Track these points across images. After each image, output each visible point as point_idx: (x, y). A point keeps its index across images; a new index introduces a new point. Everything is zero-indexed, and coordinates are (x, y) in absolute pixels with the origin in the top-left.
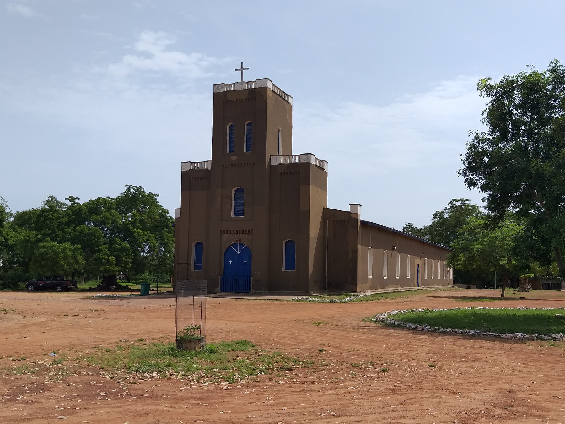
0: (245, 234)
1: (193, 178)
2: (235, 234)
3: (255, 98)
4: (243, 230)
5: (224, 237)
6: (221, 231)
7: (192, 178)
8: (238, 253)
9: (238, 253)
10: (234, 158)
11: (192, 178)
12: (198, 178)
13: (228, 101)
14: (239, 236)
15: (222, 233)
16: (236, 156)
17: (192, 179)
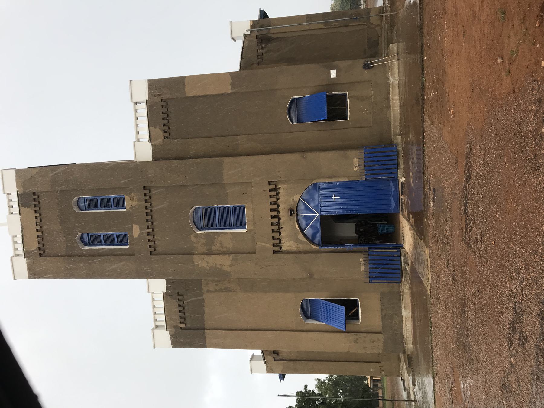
0: (278, 199)
1: (181, 323)
2: (281, 221)
3: (34, 193)
4: (271, 203)
5: (287, 245)
6: (274, 252)
7: (180, 325)
8: (318, 214)
9: (318, 214)
10: (136, 231)
11: (180, 325)
12: (180, 311)
13: (40, 249)
14: (283, 214)
15: (278, 249)
16: (133, 225)
17: (184, 325)
